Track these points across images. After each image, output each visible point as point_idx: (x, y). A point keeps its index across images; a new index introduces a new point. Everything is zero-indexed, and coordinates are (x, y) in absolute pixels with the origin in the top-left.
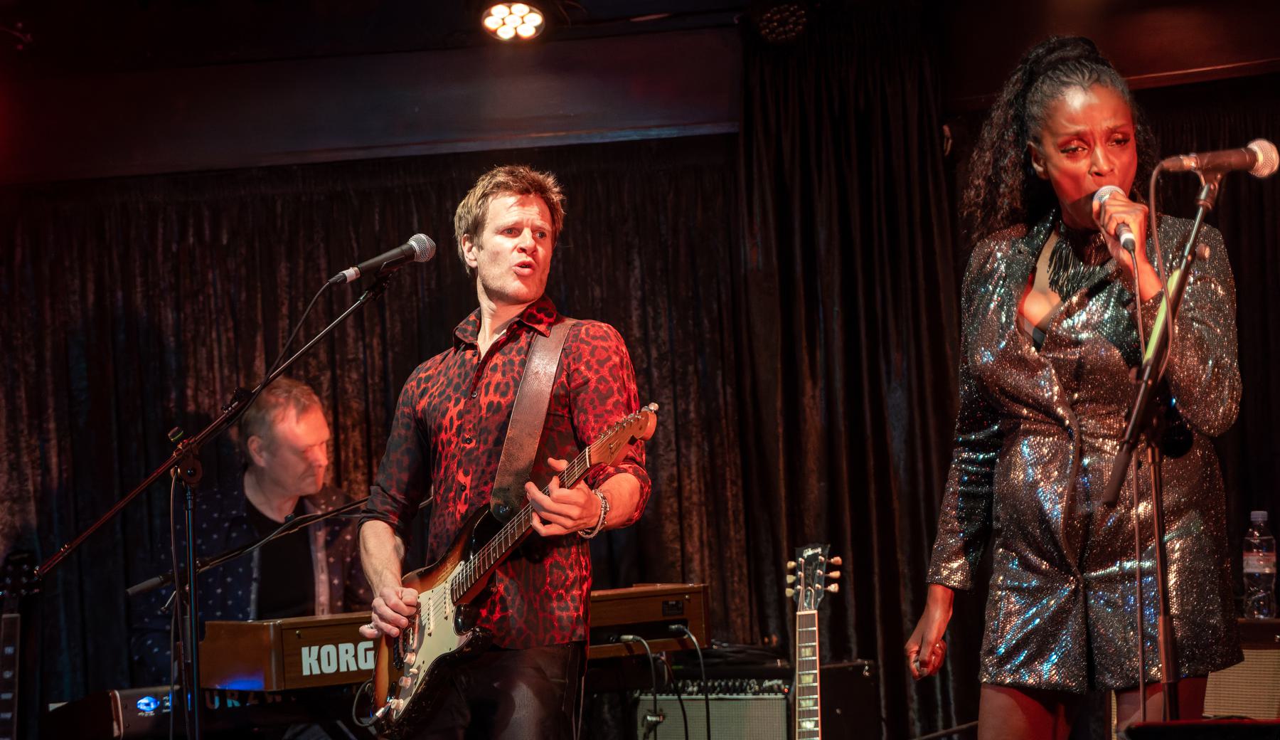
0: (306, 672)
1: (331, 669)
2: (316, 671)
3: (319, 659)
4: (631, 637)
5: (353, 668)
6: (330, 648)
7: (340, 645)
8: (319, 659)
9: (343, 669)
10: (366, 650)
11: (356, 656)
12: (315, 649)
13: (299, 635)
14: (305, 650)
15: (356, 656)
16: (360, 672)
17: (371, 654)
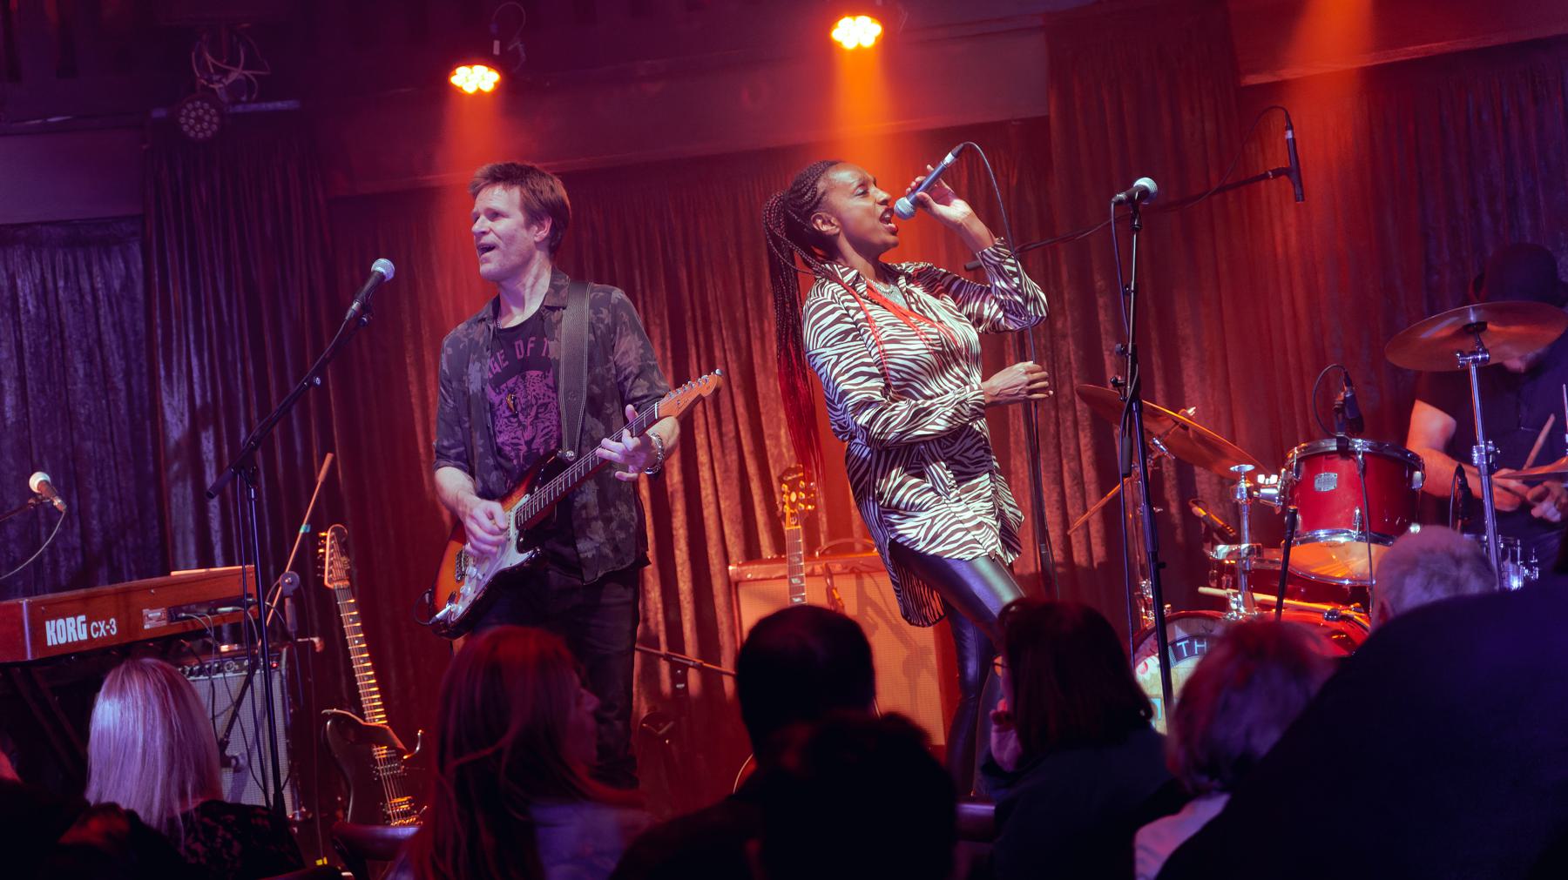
0: (49, 644)
1: (62, 641)
2: (55, 643)
3: (56, 632)
4: (229, 609)
5: (76, 639)
6: (61, 622)
7: (68, 619)
8: (56, 632)
9: (70, 640)
10: (82, 623)
11: (76, 629)
12: (53, 622)
13: (43, 612)
14: (47, 623)
15: (76, 629)
16: (80, 643)
17: (85, 626)
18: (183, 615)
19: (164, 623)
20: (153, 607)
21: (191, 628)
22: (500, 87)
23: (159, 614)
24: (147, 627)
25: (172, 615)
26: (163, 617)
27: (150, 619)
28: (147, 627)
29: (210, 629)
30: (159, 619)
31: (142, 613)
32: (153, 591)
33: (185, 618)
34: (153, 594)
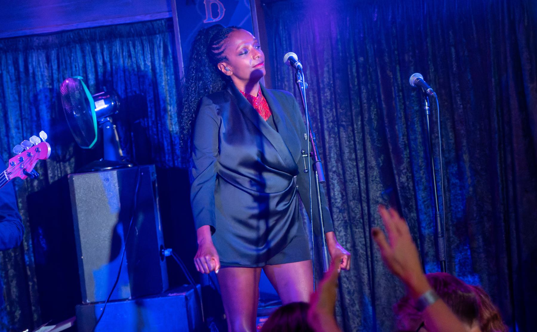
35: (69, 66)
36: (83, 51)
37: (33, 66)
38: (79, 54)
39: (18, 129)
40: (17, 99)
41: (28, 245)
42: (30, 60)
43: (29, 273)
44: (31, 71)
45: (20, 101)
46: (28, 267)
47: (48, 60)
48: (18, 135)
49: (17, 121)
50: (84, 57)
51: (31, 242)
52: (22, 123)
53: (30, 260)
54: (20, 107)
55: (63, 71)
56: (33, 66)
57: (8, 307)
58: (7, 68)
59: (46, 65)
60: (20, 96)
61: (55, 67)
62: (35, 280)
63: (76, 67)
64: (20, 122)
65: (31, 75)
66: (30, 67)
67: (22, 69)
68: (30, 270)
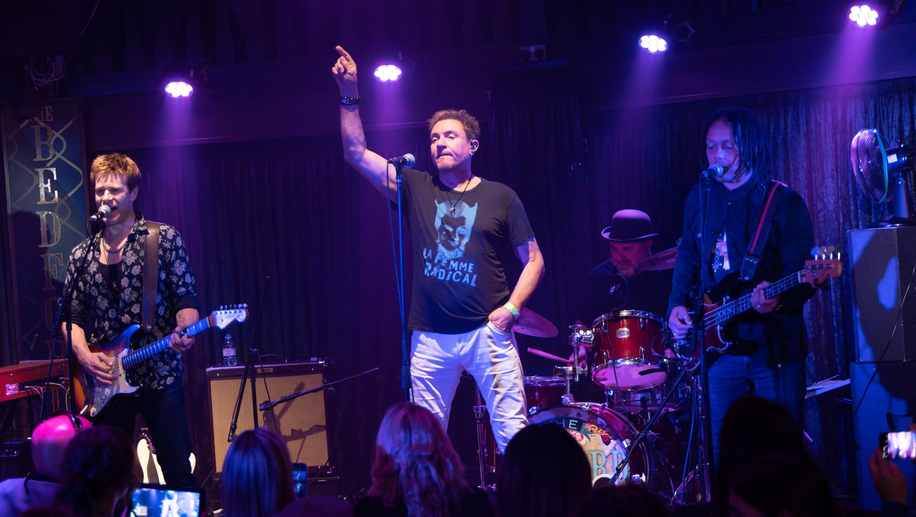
18: (27, 387)
19: (17, 392)
20: (11, 384)
21: (31, 394)
22: (193, 95)
23: (14, 387)
24: (8, 394)
25: (21, 387)
26: (16, 388)
27: (10, 390)
28: (8, 394)
29: (41, 394)
30: (14, 390)
31: (5, 387)
32: (11, 374)
33: (29, 389)
34: (11, 376)
35: (885, 116)
36: (901, 101)
37: (850, 115)
38: (897, 104)
39: (833, 178)
40: (834, 148)
41: (836, 297)
42: (848, 110)
43: (835, 324)
44: (848, 121)
45: (836, 151)
46: (834, 319)
47: (866, 111)
48: (832, 185)
49: (833, 170)
50: (901, 107)
51: (838, 294)
52: (837, 173)
53: (837, 312)
54: (836, 156)
55: (880, 122)
56: (850, 115)
57: (814, 356)
58: (826, 117)
59: (864, 115)
60: (836, 146)
61: (872, 117)
62: (841, 332)
63: (892, 117)
64: (835, 172)
65: (848, 125)
66: (848, 116)
67: (839, 118)
68: (836, 322)
